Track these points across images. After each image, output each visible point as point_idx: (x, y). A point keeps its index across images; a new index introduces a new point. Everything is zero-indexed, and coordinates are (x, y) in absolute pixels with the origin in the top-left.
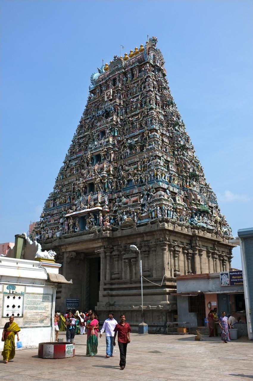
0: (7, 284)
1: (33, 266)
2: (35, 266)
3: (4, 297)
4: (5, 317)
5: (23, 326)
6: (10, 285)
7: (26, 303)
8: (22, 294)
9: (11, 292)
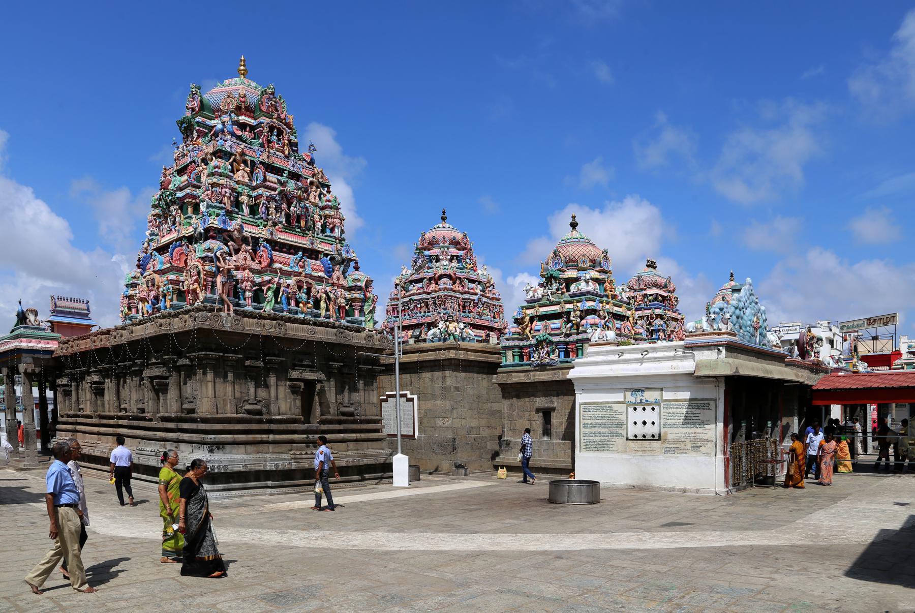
4: (631, 440)
7: (666, 417)
8: (656, 403)
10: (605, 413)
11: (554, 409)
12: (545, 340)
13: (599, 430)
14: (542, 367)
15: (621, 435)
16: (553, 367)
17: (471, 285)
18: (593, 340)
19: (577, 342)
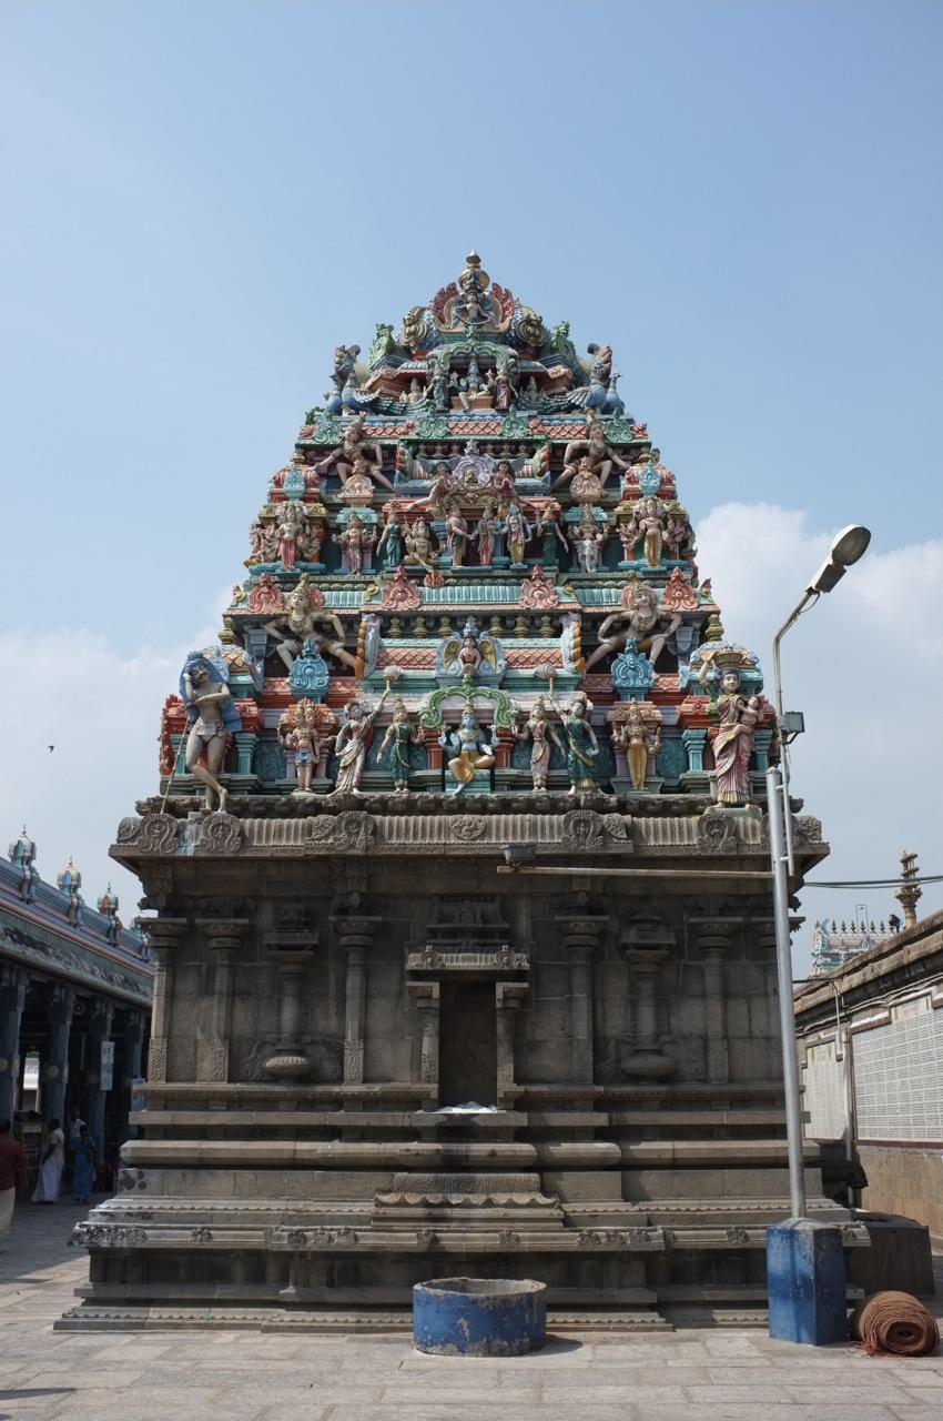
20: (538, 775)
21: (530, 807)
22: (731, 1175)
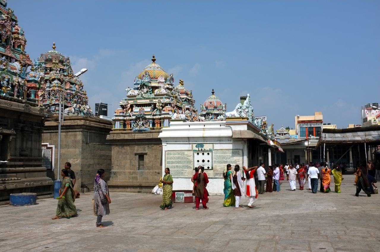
0: (195, 143)
1: (221, 126)
2: (222, 126)
3: (194, 154)
5: (214, 177)
6: (198, 144)
8: (210, 151)
9: (200, 150)
10: (180, 156)
11: (146, 154)
12: (142, 117)
13: (177, 165)
14: (140, 131)
15: (191, 168)
16: (146, 131)
17: (71, 86)
18: (173, 118)
19: (160, 119)
20: (16, 94)
21: (15, 100)
22: (36, 173)
